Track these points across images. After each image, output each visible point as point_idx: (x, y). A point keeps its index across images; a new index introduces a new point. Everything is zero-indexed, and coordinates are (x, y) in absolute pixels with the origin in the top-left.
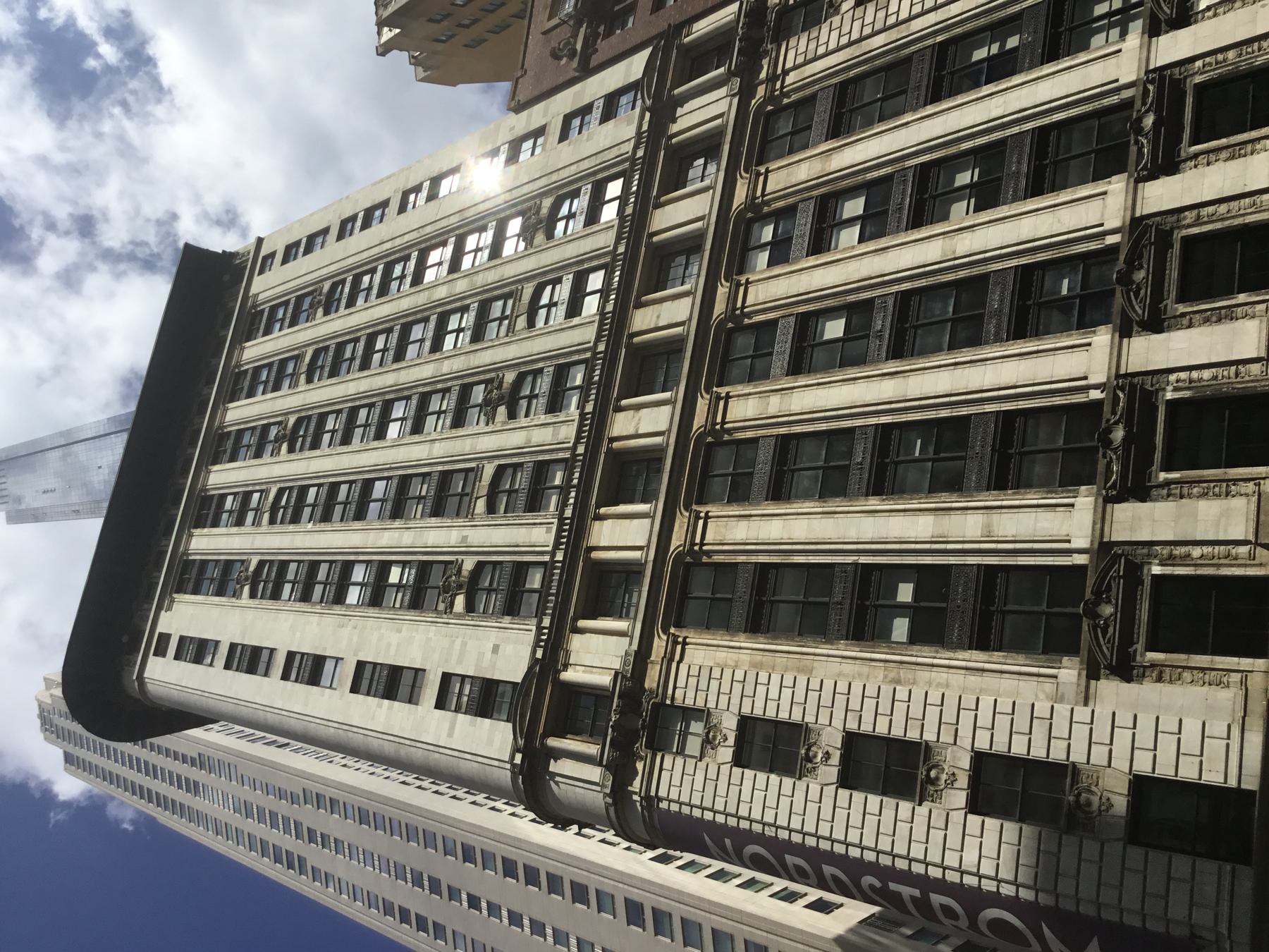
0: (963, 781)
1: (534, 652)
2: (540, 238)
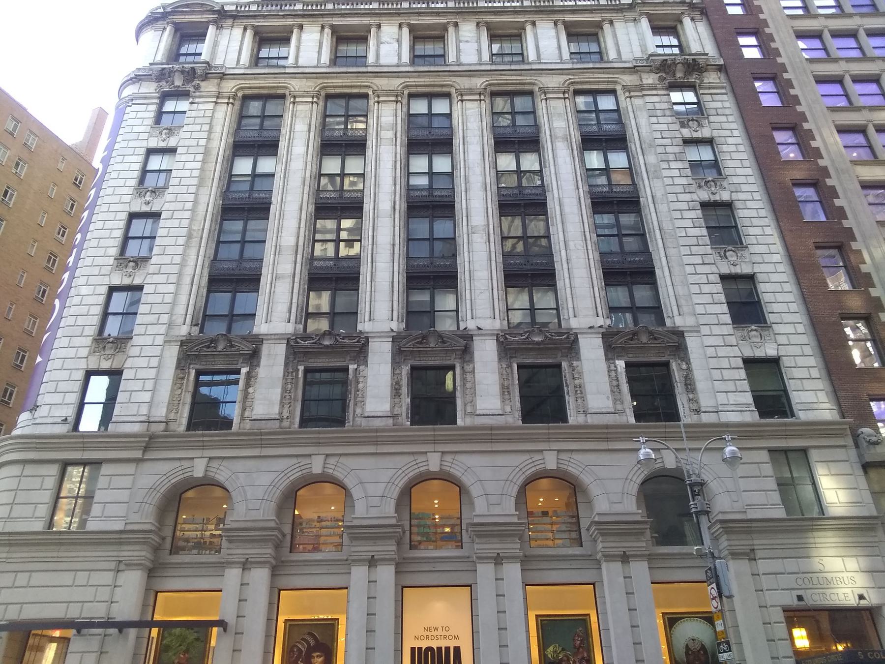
0: (127, 281)
1: (232, 4)
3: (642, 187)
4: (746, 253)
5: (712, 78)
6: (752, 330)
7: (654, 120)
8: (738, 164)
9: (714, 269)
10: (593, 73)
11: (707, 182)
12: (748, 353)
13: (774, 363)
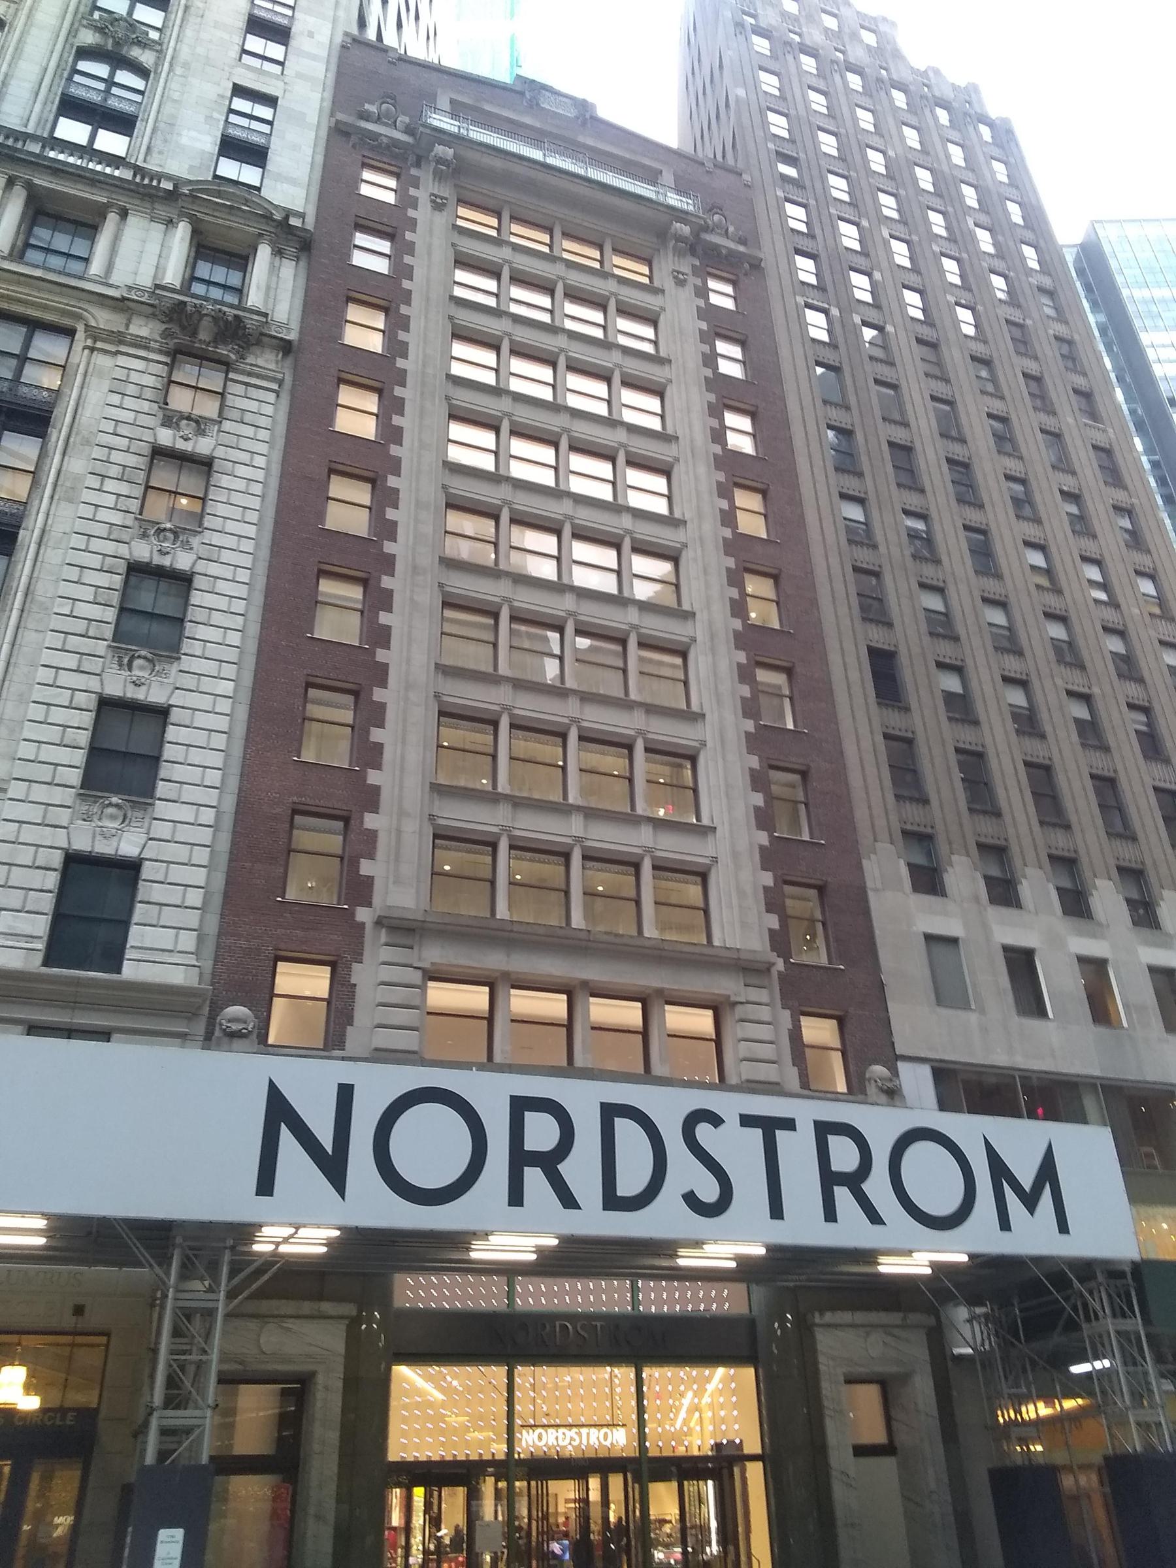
2: (88, 38)
3: (34, 513)
4: (174, 668)
5: (266, 360)
6: (111, 805)
7: (115, 399)
8: (237, 513)
9: (94, 684)
10: (39, 290)
11: (160, 531)
12: (82, 844)
13: (130, 869)
